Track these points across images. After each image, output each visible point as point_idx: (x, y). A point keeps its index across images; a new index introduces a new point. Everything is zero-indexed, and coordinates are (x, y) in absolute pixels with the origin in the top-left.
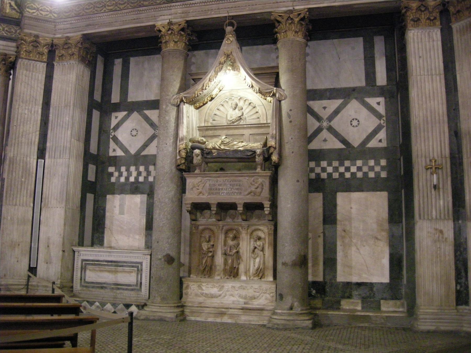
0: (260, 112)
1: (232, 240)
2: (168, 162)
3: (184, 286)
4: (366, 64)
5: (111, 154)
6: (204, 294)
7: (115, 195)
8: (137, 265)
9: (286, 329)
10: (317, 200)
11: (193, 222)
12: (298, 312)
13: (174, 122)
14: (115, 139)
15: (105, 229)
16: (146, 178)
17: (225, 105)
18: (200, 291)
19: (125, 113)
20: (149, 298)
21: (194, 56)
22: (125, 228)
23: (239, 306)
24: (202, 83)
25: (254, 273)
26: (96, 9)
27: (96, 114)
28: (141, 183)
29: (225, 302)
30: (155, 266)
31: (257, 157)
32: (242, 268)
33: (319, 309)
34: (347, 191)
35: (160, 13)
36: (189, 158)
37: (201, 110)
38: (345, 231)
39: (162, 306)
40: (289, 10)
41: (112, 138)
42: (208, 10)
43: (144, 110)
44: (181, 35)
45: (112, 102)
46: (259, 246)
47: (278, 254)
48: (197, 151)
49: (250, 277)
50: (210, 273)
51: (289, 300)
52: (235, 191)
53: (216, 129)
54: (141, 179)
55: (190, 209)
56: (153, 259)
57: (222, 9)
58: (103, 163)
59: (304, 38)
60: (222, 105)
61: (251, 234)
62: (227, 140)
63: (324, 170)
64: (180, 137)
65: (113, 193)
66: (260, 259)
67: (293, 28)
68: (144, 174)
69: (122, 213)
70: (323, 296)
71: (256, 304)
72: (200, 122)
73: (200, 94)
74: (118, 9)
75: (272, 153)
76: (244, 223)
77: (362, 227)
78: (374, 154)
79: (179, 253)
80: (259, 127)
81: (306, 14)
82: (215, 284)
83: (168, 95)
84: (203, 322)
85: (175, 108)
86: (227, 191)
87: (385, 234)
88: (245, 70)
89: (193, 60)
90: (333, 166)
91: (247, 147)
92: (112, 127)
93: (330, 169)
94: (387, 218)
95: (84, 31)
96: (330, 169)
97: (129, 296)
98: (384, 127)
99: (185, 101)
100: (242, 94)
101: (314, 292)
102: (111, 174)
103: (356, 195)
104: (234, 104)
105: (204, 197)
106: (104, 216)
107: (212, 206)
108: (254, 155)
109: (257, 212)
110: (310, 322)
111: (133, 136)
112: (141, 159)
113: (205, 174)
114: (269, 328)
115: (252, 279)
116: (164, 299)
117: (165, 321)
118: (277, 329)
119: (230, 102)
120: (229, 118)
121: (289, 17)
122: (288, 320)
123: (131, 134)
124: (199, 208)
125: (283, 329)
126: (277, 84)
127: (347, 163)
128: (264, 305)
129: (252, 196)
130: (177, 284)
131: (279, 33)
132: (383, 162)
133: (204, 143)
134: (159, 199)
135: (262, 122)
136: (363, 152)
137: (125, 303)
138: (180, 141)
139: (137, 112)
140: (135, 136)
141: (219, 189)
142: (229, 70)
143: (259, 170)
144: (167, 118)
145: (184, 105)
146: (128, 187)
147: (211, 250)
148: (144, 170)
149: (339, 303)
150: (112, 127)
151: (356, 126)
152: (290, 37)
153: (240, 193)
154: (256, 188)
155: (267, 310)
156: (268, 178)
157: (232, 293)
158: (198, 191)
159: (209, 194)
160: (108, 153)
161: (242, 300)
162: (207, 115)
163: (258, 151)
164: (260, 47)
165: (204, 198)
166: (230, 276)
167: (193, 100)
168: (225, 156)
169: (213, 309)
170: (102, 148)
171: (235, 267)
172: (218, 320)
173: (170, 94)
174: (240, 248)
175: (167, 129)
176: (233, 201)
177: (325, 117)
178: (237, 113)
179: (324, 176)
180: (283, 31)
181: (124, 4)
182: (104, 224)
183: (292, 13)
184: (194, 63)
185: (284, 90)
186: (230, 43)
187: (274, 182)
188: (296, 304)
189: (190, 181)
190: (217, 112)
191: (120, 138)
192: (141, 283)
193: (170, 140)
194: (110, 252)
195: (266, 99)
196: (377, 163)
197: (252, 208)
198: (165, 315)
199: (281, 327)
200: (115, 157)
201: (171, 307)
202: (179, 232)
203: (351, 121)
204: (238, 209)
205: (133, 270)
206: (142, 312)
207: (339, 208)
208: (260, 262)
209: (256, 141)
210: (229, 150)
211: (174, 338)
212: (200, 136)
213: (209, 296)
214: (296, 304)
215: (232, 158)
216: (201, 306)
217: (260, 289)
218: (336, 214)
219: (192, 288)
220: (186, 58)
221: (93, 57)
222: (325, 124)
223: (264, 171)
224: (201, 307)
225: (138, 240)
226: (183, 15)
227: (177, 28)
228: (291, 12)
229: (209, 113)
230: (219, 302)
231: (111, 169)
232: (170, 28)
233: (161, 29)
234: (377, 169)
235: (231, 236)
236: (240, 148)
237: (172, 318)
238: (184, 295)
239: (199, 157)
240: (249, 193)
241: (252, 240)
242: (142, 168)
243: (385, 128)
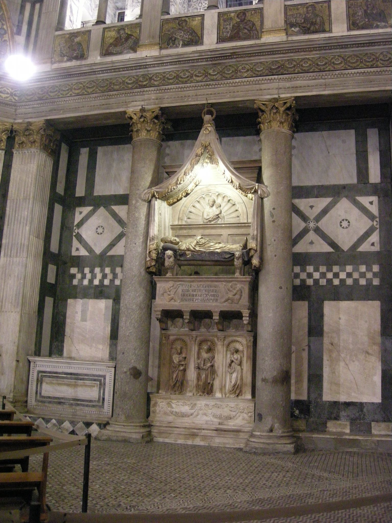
0: (240, 210)
1: (207, 353)
2: (137, 264)
3: (152, 403)
4: (358, 160)
5: (74, 253)
6: (174, 413)
7: (77, 299)
8: (100, 378)
9: (265, 454)
10: (302, 309)
11: (163, 332)
12: (279, 435)
13: (144, 219)
14: (79, 238)
15: (65, 337)
16: (112, 281)
17: (201, 201)
18: (169, 409)
19: (90, 208)
20: (112, 416)
21: (169, 147)
22: (87, 336)
23: (213, 427)
24: (176, 177)
25: (230, 389)
26: (61, 92)
27: (58, 209)
28: (107, 286)
29: (196, 422)
30: (119, 380)
31: (235, 260)
32: (217, 384)
33: (303, 431)
34: (334, 300)
35: (131, 99)
36: (160, 259)
37: (175, 207)
38: (332, 344)
39: (126, 426)
40: (274, 98)
41: (75, 236)
42: (185, 96)
43: (112, 205)
44: (155, 123)
45: (77, 195)
46: (237, 360)
47: (257, 369)
48: (169, 252)
49: (226, 395)
50: (181, 389)
51: (268, 421)
52: (211, 297)
53: (190, 229)
54: (106, 282)
55: (160, 316)
56: (117, 372)
57: (201, 95)
58: (65, 263)
59: (290, 130)
60: (198, 202)
61: (228, 345)
62: (203, 241)
63: (310, 275)
64: (151, 236)
65: (75, 297)
66: (237, 374)
67: (278, 118)
68: (110, 276)
69: (84, 319)
70: (307, 417)
71: (231, 425)
72: (173, 220)
73: (174, 189)
74: (86, 93)
75: (252, 256)
76: (220, 334)
77: (351, 339)
78: (366, 258)
79: (147, 366)
80: (239, 226)
81: (293, 103)
82: (186, 401)
83: (138, 190)
84: (172, 444)
85: (146, 204)
86: (202, 298)
87: (377, 349)
88: (224, 163)
89: (167, 151)
90: (320, 271)
91: (225, 248)
92: (76, 223)
93: (316, 275)
94: (380, 330)
95: (48, 116)
96: (316, 275)
97: (90, 413)
98: (377, 228)
99: (157, 197)
100: (220, 190)
101: (297, 412)
102: (74, 276)
103: (344, 304)
104: (212, 200)
105: (176, 303)
106: (63, 323)
107: (185, 314)
108: (232, 258)
109: (235, 321)
110: (292, 446)
111: (98, 234)
112: (107, 260)
113: (178, 278)
114: (246, 452)
115: (228, 397)
116: (128, 417)
117: (130, 442)
118: (255, 453)
119: (207, 199)
120: (205, 216)
121: (274, 106)
122: (268, 444)
123: (97, 232)
124: (170, 315)
125: (261, 453)
126: (259, 180)
127: (336, 269)
128: (241, 426)
129: (229, 303)
130: (143, 401)
131: (263, 124)
132: (376, 268)
133: (177, 243)
134: (126, 305)
135: (241, 221)
136: (353, 256)
137: (85, 421)
138: (150, 241)
139: (104, 207)
140: (101, 234)
141: (193, 295)
142: (207, 163)
143: (237, 274)
144: (137, 214)
145: (156, 201)
146: (92, 291)
148: (110, 272)
149: (325, 424)
150: (76, 223)
151: (347, 228)
152: (275, 128)
153: (217, 300)
154: (234, 295)
155: (244, 432)
156: (248, 283)
158: (170, 296)
159: (182, 300)
160: (71, 252)
161: (216, 420)
162: (181, 212)
163: (237, 254)
164: (242, 138)
165: (175, 305)
166: (203, 392)
167: (166, 196)
168: (201, 258)
169: (183, 429)
170: (63, 248)
171: (209, 383)
172: (190, 442)
173: (140, 187)
174: (215, 362)
175: (137, 227)
176: (208, 309)
177: (312, 218)
178: (214, 211)
179: (310, 282)
180: (267, 121)
181: (91, 87)
182: (64, 331)
183: (277, 102)
184: (168, 155)
185: (267, 187)
186: (208, 134)
187: (254, 289)
188: (277, 425)
189: (162, 286)
190: (193, 210)
191: (84, 236)
192: (104, 399)
193: (140, 239)
194: (69, 363)
195: (247, 196)
196: (369, 269)
197: (230, 317)
198: (130, 436)
199: (259, 451)
200: (78, 257)
201: (137, 426)
202: (148, 342)
203: (341, 222)
204: (214, 318)
205: (95, 384)
206: (103, 431)
207: (326, 319)
208: (237, 377)
209: (234, 242)
210: (205, 252)
211: (139, 462)
212: (173, 236)
213: (179, 414)
214: (277, 425)
215: (209, 261)
216: (170, 426)
217: (237, 408)
218: (323, 325)
220: (160, 150)
221: (57, 145)
222: (312, 225)
223: (244, 275)
224: (171, 427)
225: (102, 351)
226: (157, 101)
227: (150, 116)
228: (276, 100)
229: (183, 211)
230: (190, 421)
231: (73, 270)
232: (142, 116)
233: (133, 117)
234: (369, 275)
235: (205, 348)
236: (216, 250)
237: (137, 439)
238: (151, 414)
239: (172, 259)
240: (227, 301)
241: (229, 353)
242: (108, 270)
243: (378, 230)
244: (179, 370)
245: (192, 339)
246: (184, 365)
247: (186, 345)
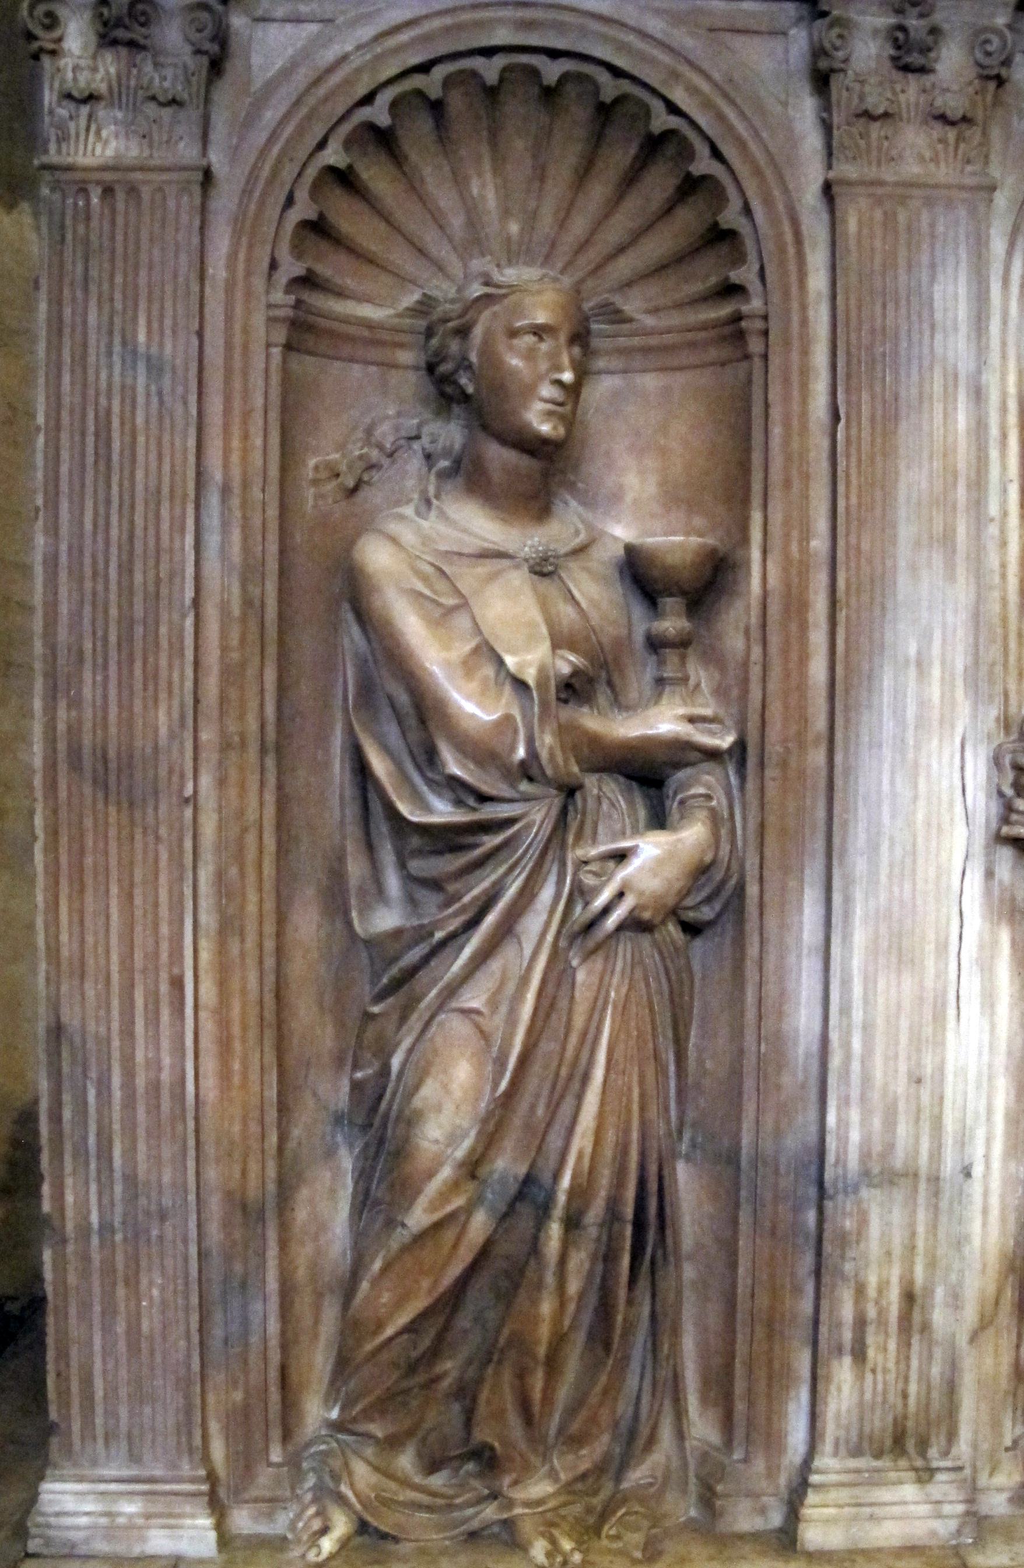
147: (664, 722)
244: (582, 933)
245: (909, 56)
246: (704, 783)
247: (719, 238)
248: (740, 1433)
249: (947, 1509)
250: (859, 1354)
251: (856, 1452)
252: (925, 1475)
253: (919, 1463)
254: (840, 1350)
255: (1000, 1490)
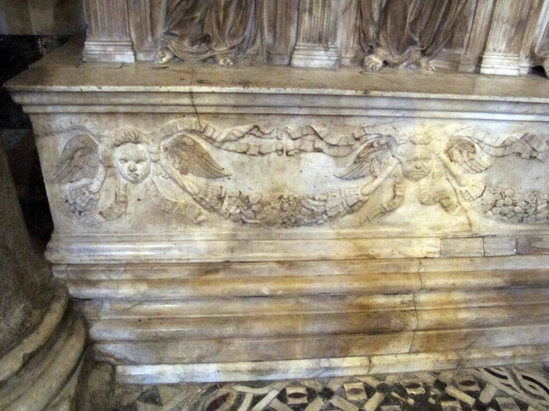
157: (445, 184)
213: (270, 213)
219: (124, 167)
248: (278, 36)
249: (332, 58)
250: (311, 12)
251: (309, 41)
252: (327, 49)
253: (326, 46)
254: (305, 11)
255: (348, 58)
